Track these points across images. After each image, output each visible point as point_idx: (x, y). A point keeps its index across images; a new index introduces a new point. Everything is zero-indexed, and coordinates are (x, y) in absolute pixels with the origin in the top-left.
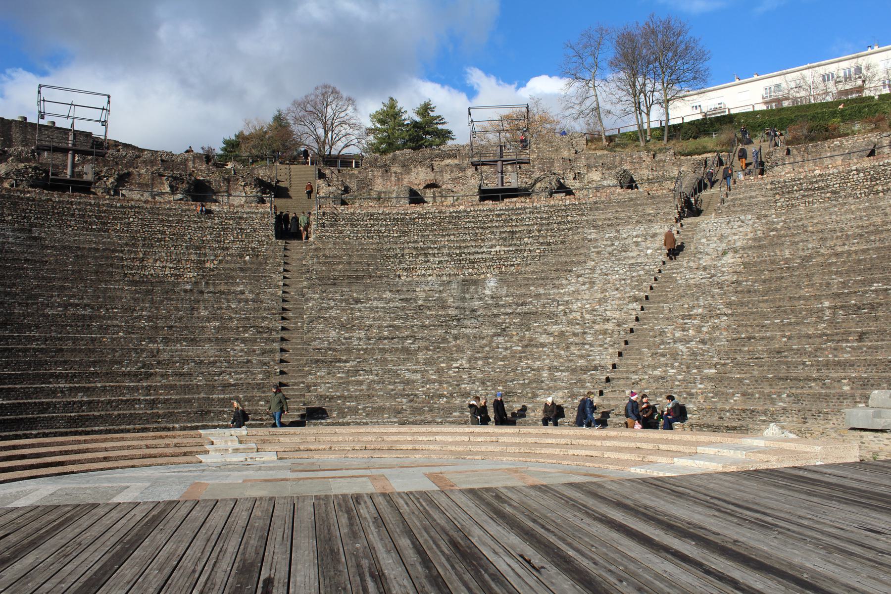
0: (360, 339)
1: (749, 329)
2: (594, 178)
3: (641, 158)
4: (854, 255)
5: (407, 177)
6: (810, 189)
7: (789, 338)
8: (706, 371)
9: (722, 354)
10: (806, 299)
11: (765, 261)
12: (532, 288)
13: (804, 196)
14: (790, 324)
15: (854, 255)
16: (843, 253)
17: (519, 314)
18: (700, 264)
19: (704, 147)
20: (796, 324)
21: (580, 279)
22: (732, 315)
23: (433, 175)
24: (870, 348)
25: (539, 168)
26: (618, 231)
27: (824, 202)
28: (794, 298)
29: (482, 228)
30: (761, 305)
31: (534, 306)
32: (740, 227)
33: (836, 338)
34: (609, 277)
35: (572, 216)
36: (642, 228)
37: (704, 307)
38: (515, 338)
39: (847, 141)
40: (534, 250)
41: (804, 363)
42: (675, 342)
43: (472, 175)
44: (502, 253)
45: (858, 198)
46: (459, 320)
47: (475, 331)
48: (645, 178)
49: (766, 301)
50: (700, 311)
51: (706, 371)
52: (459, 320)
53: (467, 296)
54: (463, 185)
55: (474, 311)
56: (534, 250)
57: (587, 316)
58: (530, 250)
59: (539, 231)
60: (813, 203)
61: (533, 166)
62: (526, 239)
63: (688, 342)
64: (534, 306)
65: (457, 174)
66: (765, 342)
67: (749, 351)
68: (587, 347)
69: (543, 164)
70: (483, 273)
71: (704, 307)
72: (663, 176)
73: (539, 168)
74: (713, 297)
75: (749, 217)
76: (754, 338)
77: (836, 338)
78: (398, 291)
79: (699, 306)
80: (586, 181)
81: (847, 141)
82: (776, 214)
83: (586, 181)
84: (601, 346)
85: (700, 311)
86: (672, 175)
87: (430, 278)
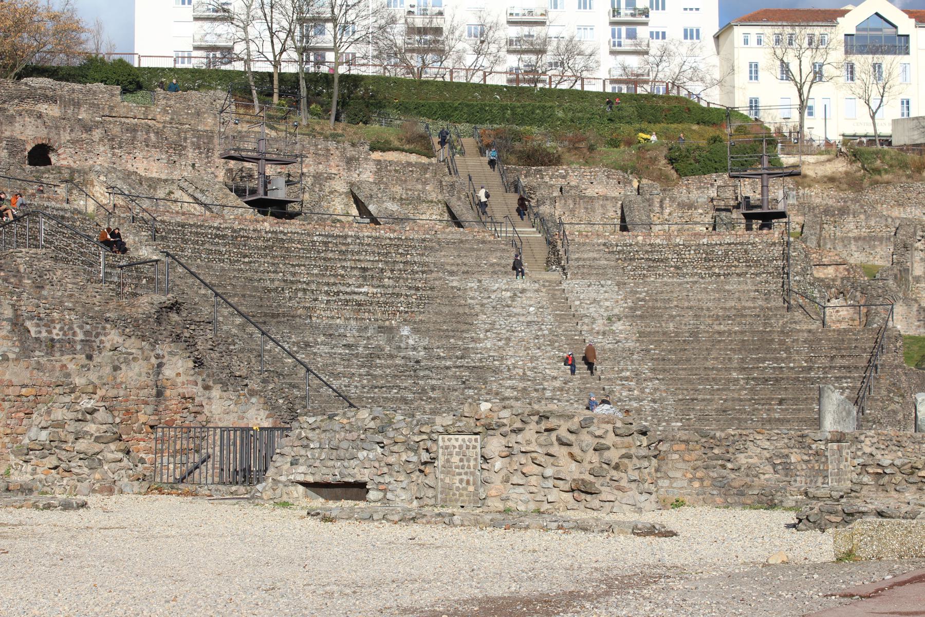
0: (356, 387)
1: (685, 392)
2: (337, 188)
3: (328, 150)
4: (733, 335)
5: (9, 128)
6: (650, 260)
7: (725, 400)
8: (673, 424)
9: (678, 411)
10: (718, 370)
11: (658, 332)
12: (452, 340)
13: (649, 267)
14: (718, 390)
15: (733, 335)
16: (724, 332)
17: (468, 367)
18: (593, 329)
19: (387, 142)
20: (723, 390)
21: (488, 333)
22: (663, 379)
23: (46, 131)
24: (794, 410)
25: (193, 143)
26: (480, 281)
27: (673, 277)
28: (708, 368)
29: (324, 259)
30: (681, 372)
31: (472, 360)
32: (606, 292)
33: (762, 402)
34: (516, 334)
35: (412, 255)
36: (505, 281)
37: (632, 371)
38: (483, 392)
39: (573, 172)
40: (411, 296)
41: (752, 419)
42: (630, 400)
43: (101, 140)
44: (379, 295)
45: (702, 278)
46: (415, 371)
47: (439, 382)
48: (398, 197)
49: (685, 369)
50: (628, 373)
51: (673, 424)
52: (415, 371)
53: (402, 345)
54: (88, 152)
55: (418, 362)
56: (411, 296)
57: (529, 373)
58: (407, 295)
59: (392, 271)
60: (663, 276)
61: (185, 139)
62: (386, 280)
63: (641, 401)
64: (472, 360)
65: (79, 134)
66: (705, 403)
67: (701, 410)
68: (555, 401)
69: (199, 138)
70: (388, 320)
71: (632, 371)
72: (419, 198)
73: (193, 143)
74: (632, 361)
75: (609, 282)
76: (696, 399)
77: (762, 402)
78: (331, 335)
79: (627, 370)
80: (327, 190)
81: (573, 172)
82: (635, 283)
83: (327, 190)
84: (567, 401)
85: (628, 373)
86: (430, 198)
87: (338, 321)
